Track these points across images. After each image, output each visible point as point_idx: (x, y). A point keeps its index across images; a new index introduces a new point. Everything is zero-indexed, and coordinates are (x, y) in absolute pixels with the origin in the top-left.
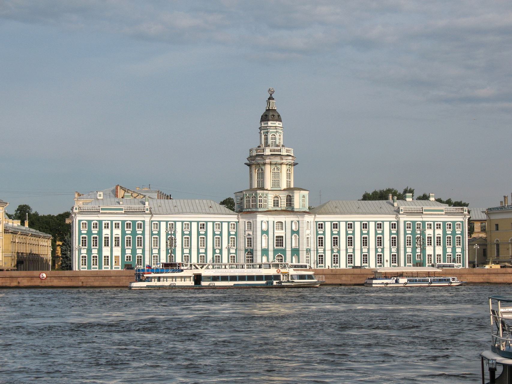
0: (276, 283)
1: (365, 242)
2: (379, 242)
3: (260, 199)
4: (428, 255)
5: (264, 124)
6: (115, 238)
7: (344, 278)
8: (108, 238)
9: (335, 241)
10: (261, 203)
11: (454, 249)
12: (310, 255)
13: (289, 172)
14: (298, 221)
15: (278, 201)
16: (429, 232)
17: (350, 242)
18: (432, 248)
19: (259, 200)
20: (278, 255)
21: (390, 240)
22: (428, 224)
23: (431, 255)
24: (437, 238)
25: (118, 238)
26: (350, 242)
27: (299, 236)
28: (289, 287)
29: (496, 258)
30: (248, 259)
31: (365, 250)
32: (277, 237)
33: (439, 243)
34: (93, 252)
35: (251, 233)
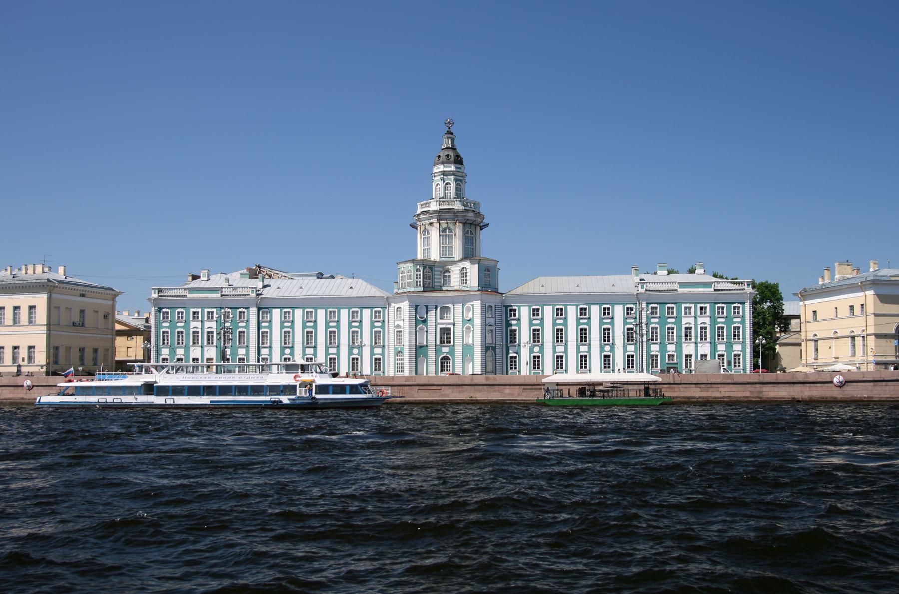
0: (289, 399)
1: (583, 335)
2: (607, 335)
3: (418, 273)
4: (687, 356)
5: (436, 169)
6: (208, 332)
7: (508, 390)
8: (198, 332)
9: (536, 335)
10: (418, 280)
11: (729, 346)
12: (496, 356)
13: (469, 235)
14: (473, 305)
15: (449, 276)
16: (687, 321)
17: (560, 336)
18: (693, 345)
19: (417, 275)
20: (444, 357)
21: (624, 333)
22: (686, 308)
23: (690, 356)
24: (701, 328)
25: (212, 332)
26: (560, 336)
27: (473, 328)
28: (468, 404)
29: (813, 361)
30: (398, 362)
31: (584, 349)
32: (440, 329)
33: (703, 338)
34: (178, 353)
35: (401, 323)
